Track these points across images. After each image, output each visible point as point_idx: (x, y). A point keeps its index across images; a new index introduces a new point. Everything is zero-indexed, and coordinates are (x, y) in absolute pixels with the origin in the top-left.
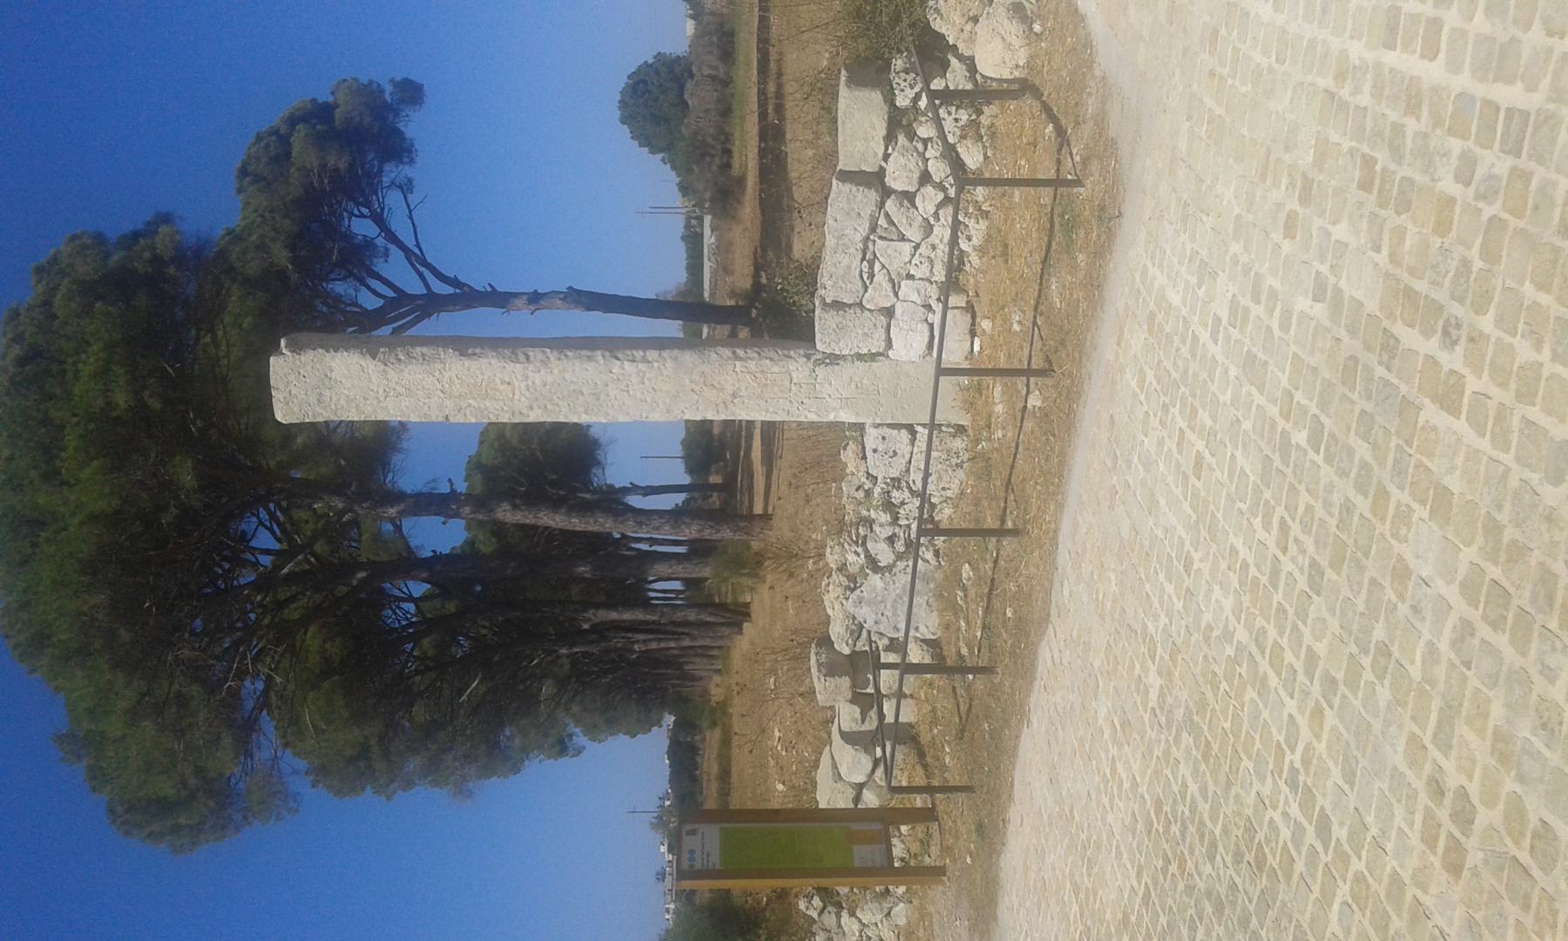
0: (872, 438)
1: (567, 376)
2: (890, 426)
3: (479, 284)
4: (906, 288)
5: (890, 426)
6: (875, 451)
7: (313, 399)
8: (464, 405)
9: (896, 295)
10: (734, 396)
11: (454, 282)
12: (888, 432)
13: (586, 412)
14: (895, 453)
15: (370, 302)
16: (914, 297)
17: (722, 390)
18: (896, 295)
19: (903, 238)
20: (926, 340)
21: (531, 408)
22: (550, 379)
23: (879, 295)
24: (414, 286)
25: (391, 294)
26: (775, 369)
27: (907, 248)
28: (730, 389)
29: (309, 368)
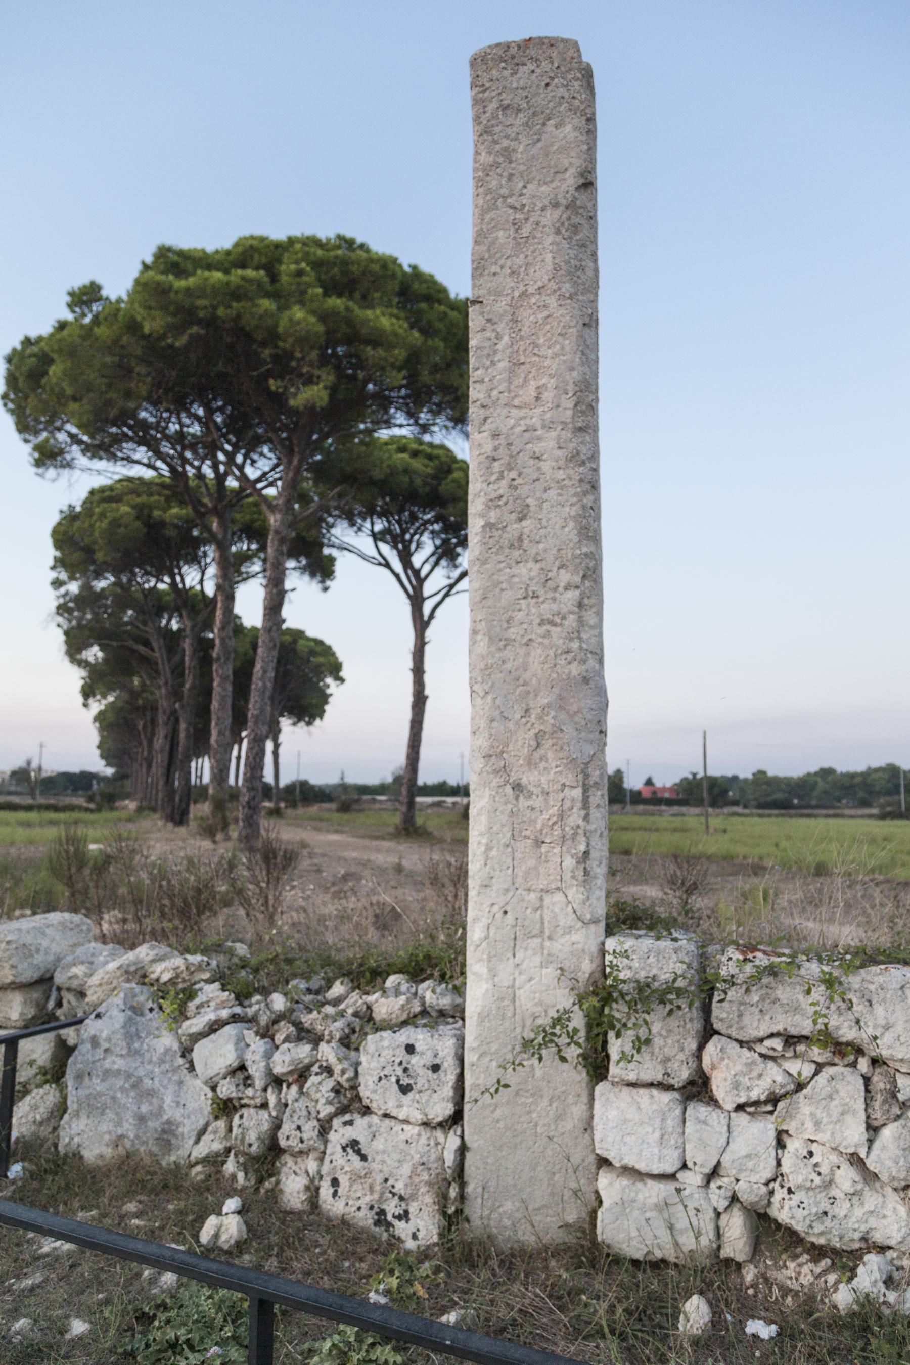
0: (435, 1044)
1: (553, 493)
2: (461, 1077)
3: (429, 634)
4: (755, 1134)
5: (461, 1077)
6: (410, 1049)
7: (507, 99)
8: (500, 327)
9: (740, 1108)
10: (518, 787)
11: (432, 616)
12: (449, 1077)
13: (489, 526)
14: (405, 1089)
15: (417, 560)
16: (739, 1147)
17: (530, 763)
18: (740, 1108)
19: (873, 1130)
20: (642, 1167)
21: (495, 435)
22: (546, 466)
23: (728, 1069)
24: (429, 588)
25: (423, 573)
26: (569, 862)
27: (853, 1134)
28: (528, 778)
29: (562, 91)
